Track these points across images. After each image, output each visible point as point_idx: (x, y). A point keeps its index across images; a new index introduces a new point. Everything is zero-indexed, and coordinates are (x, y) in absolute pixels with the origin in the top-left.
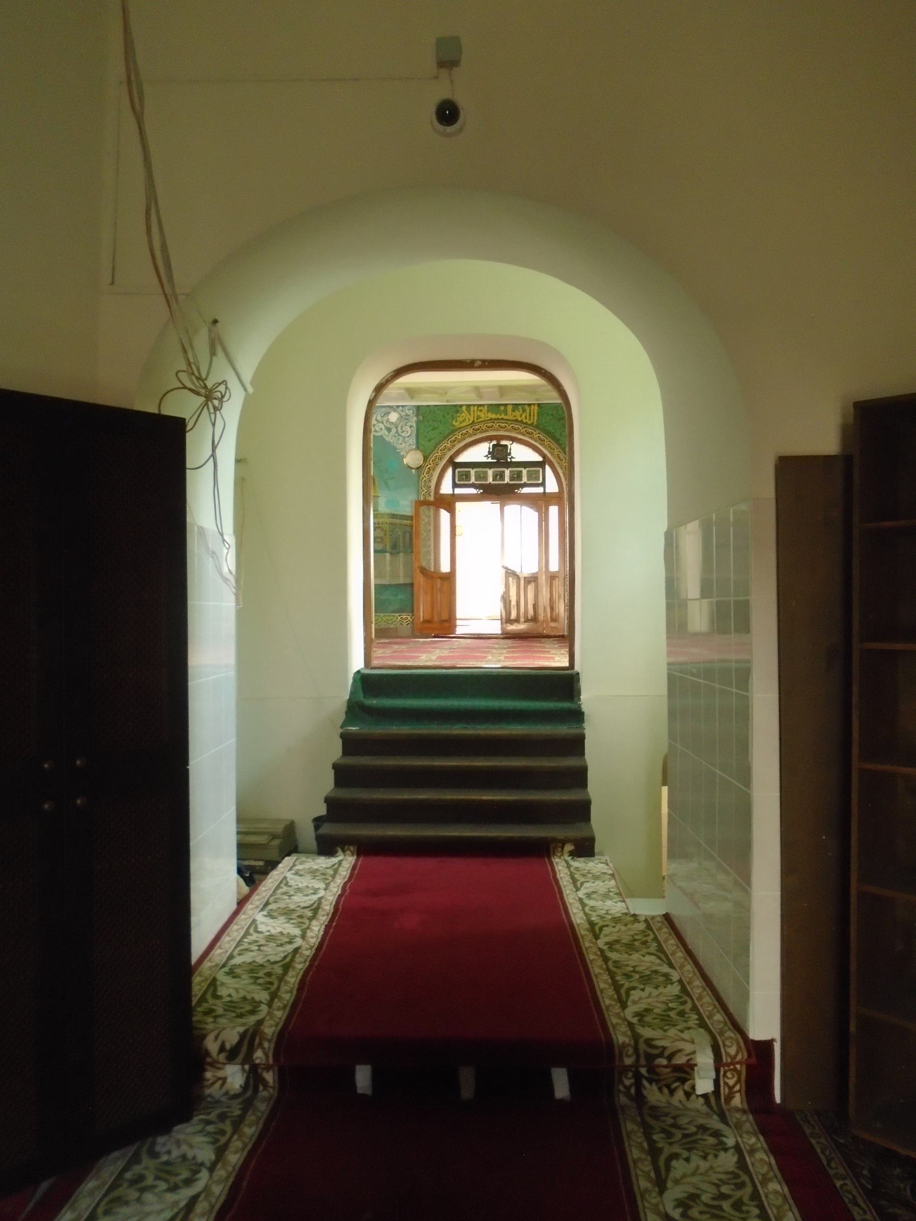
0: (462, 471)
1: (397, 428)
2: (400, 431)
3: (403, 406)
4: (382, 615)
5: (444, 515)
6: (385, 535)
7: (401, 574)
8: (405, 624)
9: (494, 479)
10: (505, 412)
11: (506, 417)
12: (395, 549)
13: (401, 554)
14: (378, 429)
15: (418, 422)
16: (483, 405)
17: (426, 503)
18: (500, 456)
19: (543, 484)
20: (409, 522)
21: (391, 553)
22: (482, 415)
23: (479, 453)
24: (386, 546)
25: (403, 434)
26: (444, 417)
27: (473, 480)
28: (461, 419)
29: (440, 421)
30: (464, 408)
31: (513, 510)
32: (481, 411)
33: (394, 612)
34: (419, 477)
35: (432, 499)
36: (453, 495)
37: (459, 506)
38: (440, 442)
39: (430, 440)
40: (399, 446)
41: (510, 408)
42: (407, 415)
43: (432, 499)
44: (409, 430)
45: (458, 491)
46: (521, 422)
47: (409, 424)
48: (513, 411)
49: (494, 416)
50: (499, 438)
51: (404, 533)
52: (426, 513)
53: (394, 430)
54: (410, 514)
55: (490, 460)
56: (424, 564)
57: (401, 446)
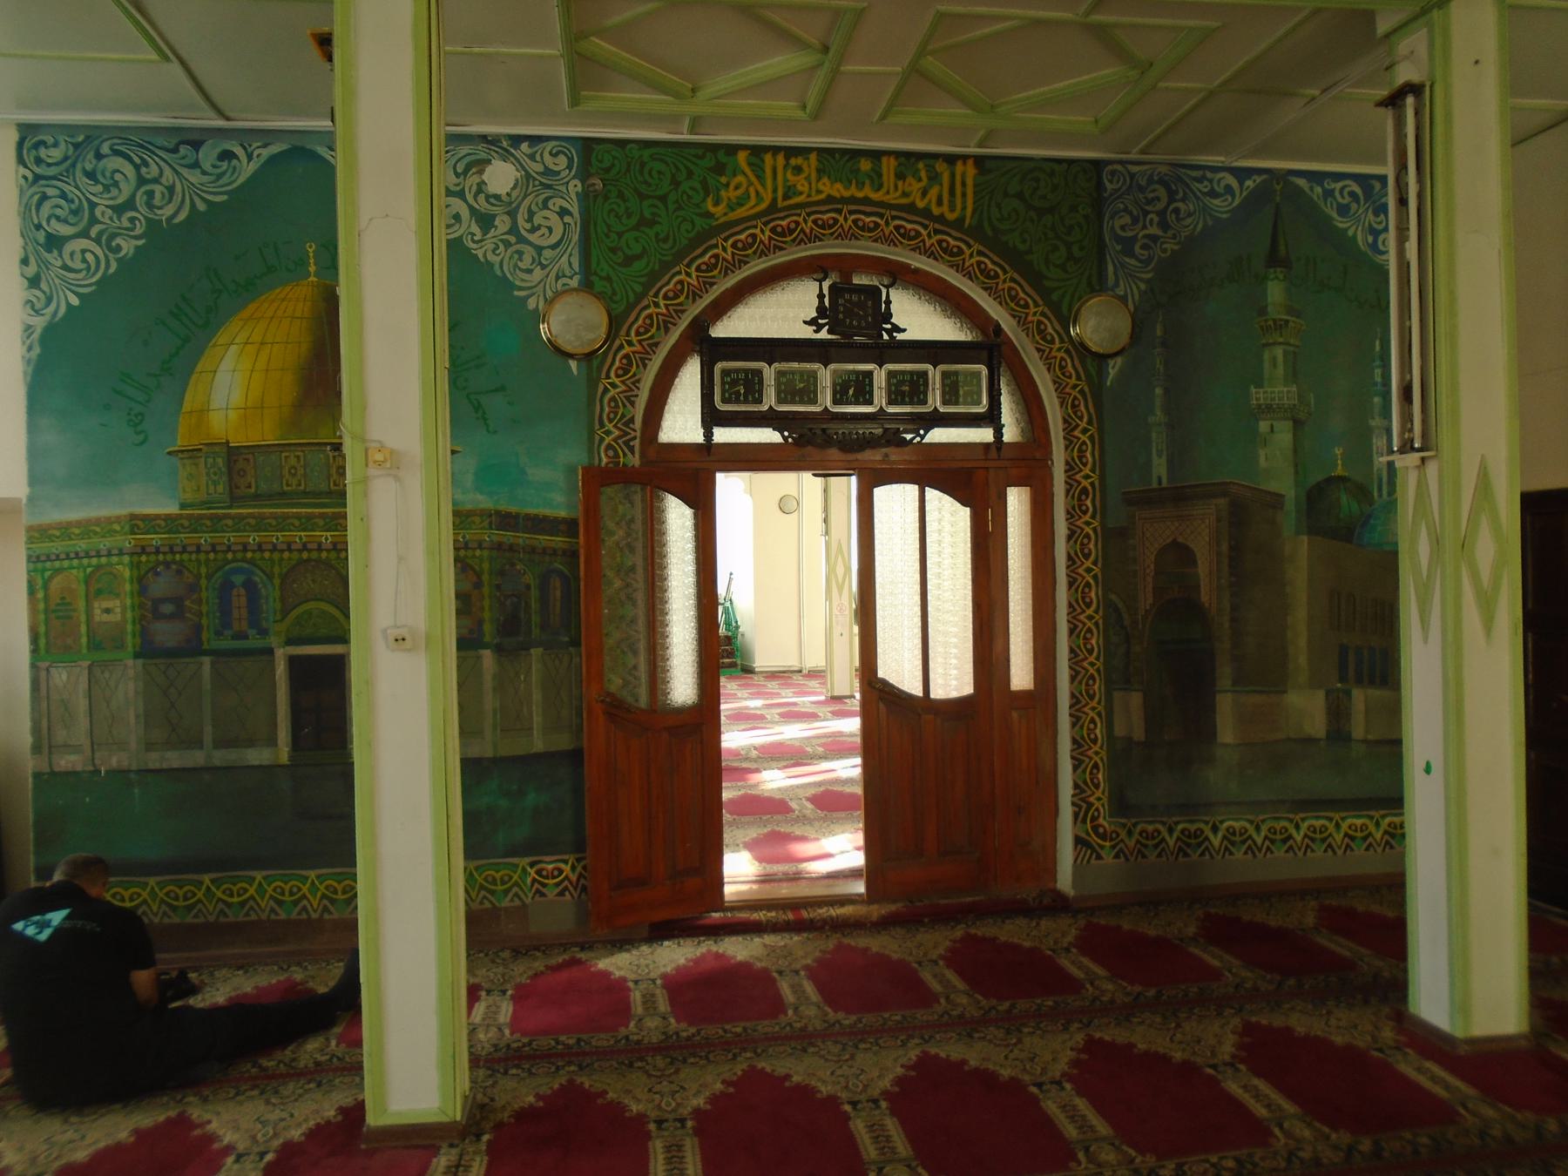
0: (736, 374)
1: (512, 214)
3: (535, 140)
5: (678, 517)
6: (478, 585)
7: (537, 720)
8: (551, 893)
9: (840, 397)
10: (876, 179)
11: (874, 196)
13: (536, 652)
15: (586, 197)
16: (803, 151)
17: (616, 475)
18: (855, 322)
19: (992, 418)
20: (559, 541)
21: (499, 650)
22: (803, 186)
23: (785, 312)
24: (480, 622)
25: (531, 238)
26: (676, 184)
27: (770, 400)
28: (733, 194)
29: (663, 199)
30: (742, 156)
31: (895, 503)
32: (798, 170)
34: (592, 382)
35: (635, 461)
36: (708, 446)
37: (730, 488)
38: (666, 267)
39: (629, 261)
41: (889, 166)
42: (548, 172)
43: (635, 461)
44: (556, 225)
45: (722, 435)
46: (926, 213)
48: (900, 176)
49: (838, 190)
50: (847, 265)
52: (617, 504)
53: (502, 224)
54: (562, 514)
55: (824, 334)
56: (614, 683)
57: (530, 280)
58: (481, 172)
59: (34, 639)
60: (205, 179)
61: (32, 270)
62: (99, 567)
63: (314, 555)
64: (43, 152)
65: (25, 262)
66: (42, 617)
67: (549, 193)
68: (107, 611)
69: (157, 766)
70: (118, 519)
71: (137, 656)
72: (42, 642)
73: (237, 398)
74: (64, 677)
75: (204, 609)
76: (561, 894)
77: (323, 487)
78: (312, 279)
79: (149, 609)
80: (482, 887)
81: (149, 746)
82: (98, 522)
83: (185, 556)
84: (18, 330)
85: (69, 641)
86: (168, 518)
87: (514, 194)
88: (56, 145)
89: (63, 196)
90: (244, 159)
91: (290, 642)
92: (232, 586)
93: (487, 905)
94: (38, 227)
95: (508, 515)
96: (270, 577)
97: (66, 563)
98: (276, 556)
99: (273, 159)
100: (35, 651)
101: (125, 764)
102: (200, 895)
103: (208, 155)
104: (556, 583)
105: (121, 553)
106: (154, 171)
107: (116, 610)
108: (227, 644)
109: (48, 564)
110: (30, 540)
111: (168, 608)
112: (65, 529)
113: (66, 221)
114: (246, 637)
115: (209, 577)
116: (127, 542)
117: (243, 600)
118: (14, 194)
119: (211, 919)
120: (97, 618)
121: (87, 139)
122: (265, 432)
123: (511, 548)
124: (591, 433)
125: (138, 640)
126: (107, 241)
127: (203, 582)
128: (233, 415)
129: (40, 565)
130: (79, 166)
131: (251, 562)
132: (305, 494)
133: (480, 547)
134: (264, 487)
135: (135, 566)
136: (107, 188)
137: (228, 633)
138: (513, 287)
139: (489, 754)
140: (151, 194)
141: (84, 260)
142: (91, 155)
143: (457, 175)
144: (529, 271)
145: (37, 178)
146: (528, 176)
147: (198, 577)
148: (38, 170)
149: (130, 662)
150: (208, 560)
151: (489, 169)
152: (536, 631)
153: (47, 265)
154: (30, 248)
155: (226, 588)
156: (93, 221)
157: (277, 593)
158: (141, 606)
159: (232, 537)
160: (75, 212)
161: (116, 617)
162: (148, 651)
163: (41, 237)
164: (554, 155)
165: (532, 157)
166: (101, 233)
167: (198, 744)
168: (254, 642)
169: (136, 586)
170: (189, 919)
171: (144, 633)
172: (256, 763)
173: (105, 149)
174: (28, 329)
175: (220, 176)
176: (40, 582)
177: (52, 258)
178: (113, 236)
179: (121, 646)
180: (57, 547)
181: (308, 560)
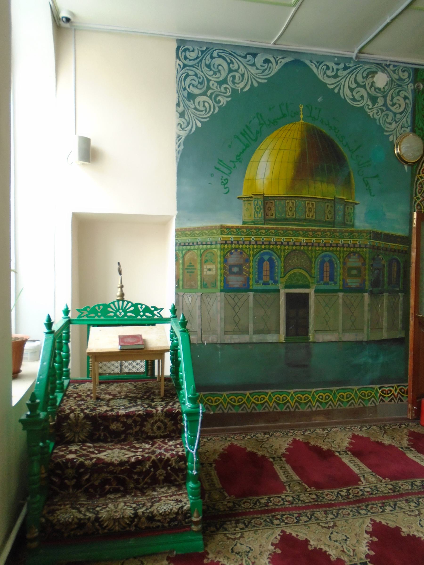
1: (385, 97)
2: (389, 102)
4: (356, 388)
6: (364, 264)
7: (385, 324)
8: (387, 400)
12: (376, 289)
13: (386, 295)
14: (357, 97)
15: (416, 92)
21: (371, 293)
24: (365, 280)
25: (393, 109)
33: (372, 383)
40: (386, 127)
42: (400, 79)
44: (402, 103)
47: (403, 94)
51: (390, 265)
53: (381, 101)
58: (373, 77)
59: (177, 282)
60: (258, 71)
61: (181, 109)
62: (206, 249)
63: (298, 248)
64: (188, 53)
65: (178, 105)
66: (181, 272)
67: (400, 88)
68: (210, 270)
69: (229, 341)
70: (215, 228)
71: (222, 291)
72: (181, 283)
73: (268, 174)
74: (190, 299)
75: (251, 270)
76: (390, 401)
77: (303, 217)
78: (302, 121)
79: (228, 269)
80: (360, 398)
81: (226, 332)
82: (207, 228)
83: (244, 246)
84: (174, 137)
85: (193, 283)
86: (237, 228)
87: (386, 88)
88: (193, 51)
89: (196, 75)
90: (274, 64)
91: (287, 287)
92: (264, 260)
93: (361, 405)
94: (185, 89)
95: (377, 233)
96: (280, 257)
97: (192, 247)
98: (283, 247)
99: (286, 64)
100: (177, 287)
101: (215, 340)
102: (245, 400)
103: (259, 60)
104: (395, 264)
105: (216, 244)
106: (235, 66)
107: (213, 270)
108: (260, 287)
109: (184, 247)
110: (177, 236)
111: (235, 270)
112: (192, 231)
113: (197, 87)
114: (268, 284)
115: (254, 256)
116: (219, 238)
117: (268, 267)
118: (175, 72)
119: (249, 411)
120: (205, 273)
121: (208, 49)
122: (279, 190)
123: (378, 248)
124: (412, 198)
125: (222, 284)
126: (214, 97)
127: (251, 258)
128: (266, 182)
129: (181, 247)
130: (203, 61)
131: (272, 250)
132: (295, 220)
133: (366, 247)
134: (278, 216)
135: (222, 249)
136: (215, 73)
137: (261, 282)
138: (383, 130)
139: (365, 339)
140: (234, 77)
141: (204, 106)
142: (208, 57)
143: (363, 78)
144: (391, 124)
145: (185, 66)
146: (392, 80)
147: (249, 256)
148: (186, 62)
149: (219, 294)
150: (253, 248)
151: (376, 76)
152: (386, 286)
153: (188, 107)
154: (181, 99)
155: (261, 261)
156: (209, 88)
157: (282, 264)
158: (224, 268)
159: (263, 238)
160: (201, 83)
161: (213, 273)
162: (227, 289)
163: (186, 95)
164: (403, 71)
165: (394, 71)
166: (211, 94)
167: (246, 332)
168: (271, 286)
169: (222, 259)
170: (240, 411)
171: (225, 281)
172: (270, 341)
173: (215, 54)
174: (179, 136)
175: (264, 71)
176: (181, 255)
177: (190, 103)
178: (217, 96)
179: (215, 286)
180: (189, 239)
181: (296, 250)
